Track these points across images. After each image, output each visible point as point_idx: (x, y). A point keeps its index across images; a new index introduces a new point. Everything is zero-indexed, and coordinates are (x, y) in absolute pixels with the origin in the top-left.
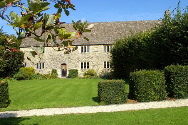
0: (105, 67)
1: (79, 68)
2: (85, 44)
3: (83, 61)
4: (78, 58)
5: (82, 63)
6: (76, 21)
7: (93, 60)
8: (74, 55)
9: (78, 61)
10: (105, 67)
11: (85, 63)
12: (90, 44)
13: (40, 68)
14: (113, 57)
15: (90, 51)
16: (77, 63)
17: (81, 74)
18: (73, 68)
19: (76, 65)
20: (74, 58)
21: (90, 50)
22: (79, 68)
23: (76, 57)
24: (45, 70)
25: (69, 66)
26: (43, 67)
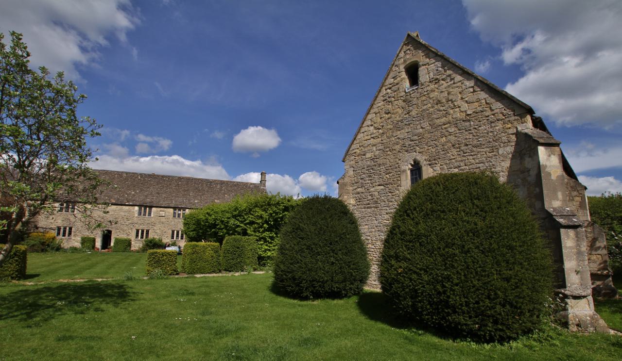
0: (173, 237)
1: (132, 237)
2: (145, 205)
3: (141, 227)
4: (133, 223)
5: (138, 231)
6: (64, 73)
7: (155, 228)
8: (127, 218)
9: (132, 227)
10: (173, 237)
11: (143, 231)
12: (154, 205)
13: (64, 235)
14: (275, 277)
15: (152, 216)
16: (130, 231)
17: (137, 245)
18: (123, 236)
19: (128, 234)
20: (125, 222)
21: (152, 213)
22: (132, 237)
23: (130, 222)
24: (73, 238)
25: (117, 234)
26: (70, 234)
